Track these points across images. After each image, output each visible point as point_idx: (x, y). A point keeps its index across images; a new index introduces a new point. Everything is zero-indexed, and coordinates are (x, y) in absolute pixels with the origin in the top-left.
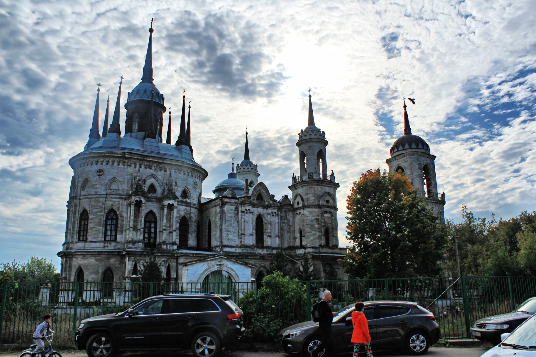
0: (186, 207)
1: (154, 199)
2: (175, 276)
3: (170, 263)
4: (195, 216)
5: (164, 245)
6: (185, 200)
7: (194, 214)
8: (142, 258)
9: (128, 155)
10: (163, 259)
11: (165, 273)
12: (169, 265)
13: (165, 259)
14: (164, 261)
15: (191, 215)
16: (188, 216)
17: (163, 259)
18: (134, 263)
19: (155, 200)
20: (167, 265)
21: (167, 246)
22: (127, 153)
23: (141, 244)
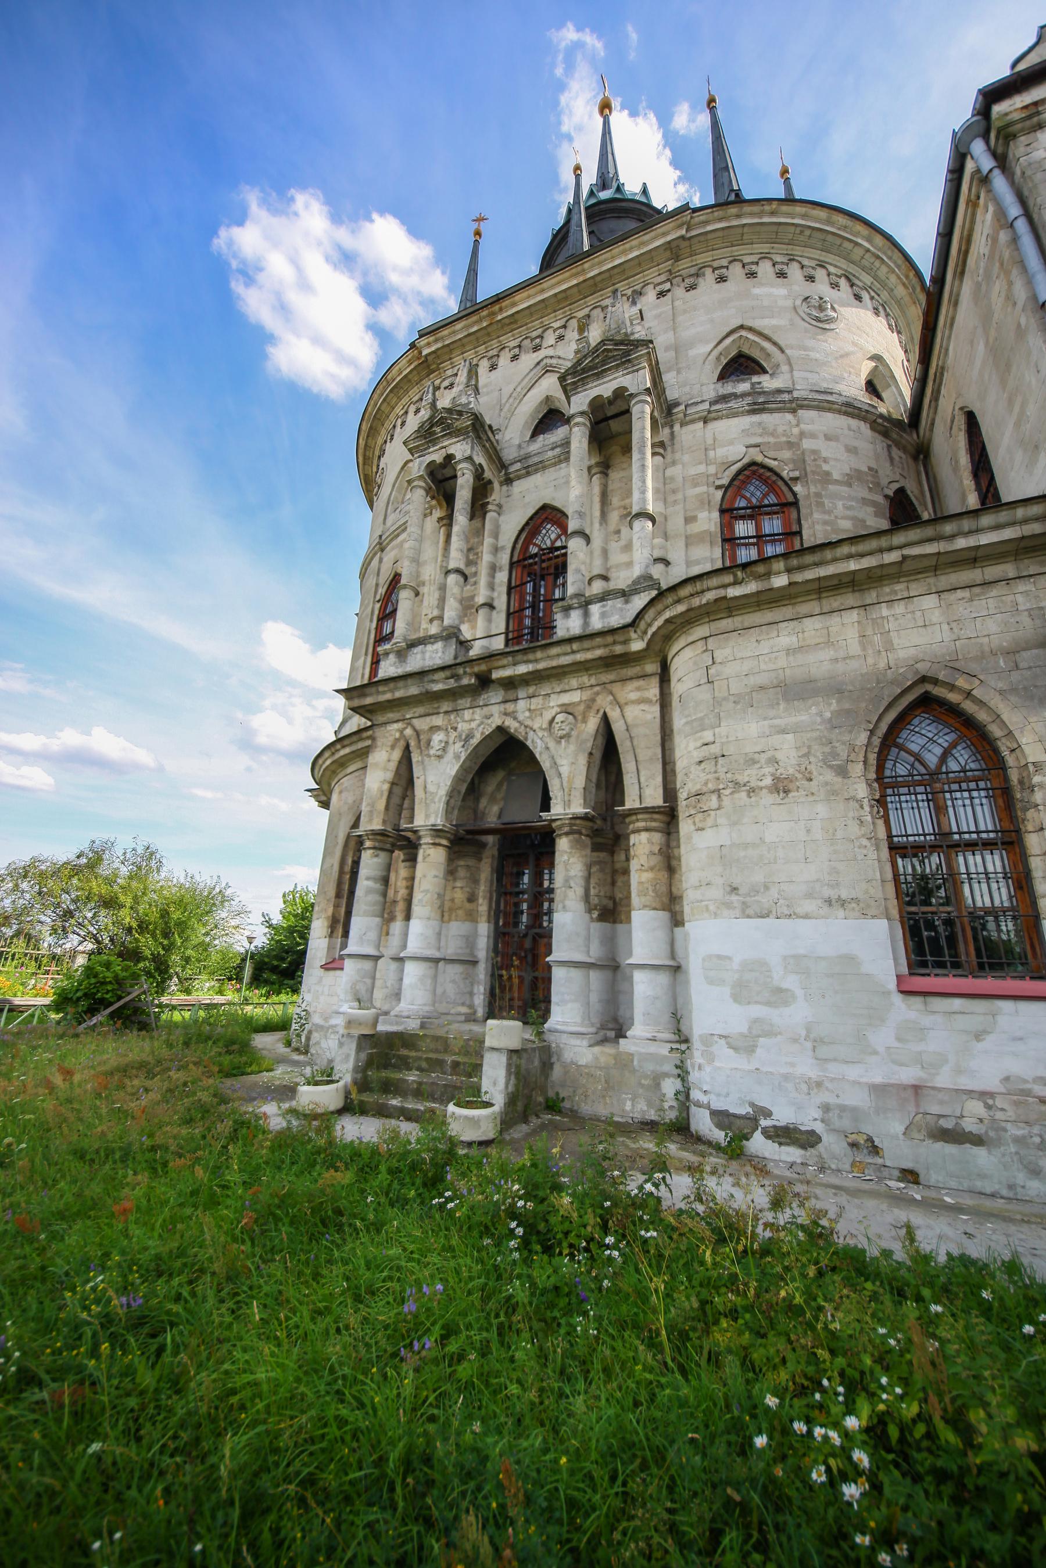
0: (756, 418)
1: (553, 449)
2: (654, 797)
3: (614, 714)
4: (852, 450)
5: (567, 609)
6: (744, 387)
7: (828, 438)
8: (438, 721)
9: (429, 344)
10: (566, 698)
11: (580, 782)
12: (606, 720)
13: (575, 697)
14: (567, 709)
15: (807, 444)
16: (786, 454)
17: (566, 698)
18: (397, 755)
19: (558, 450)
20: (593, 723)
21: (586, 615)
22: (423, 342)
23: (439, 645)
